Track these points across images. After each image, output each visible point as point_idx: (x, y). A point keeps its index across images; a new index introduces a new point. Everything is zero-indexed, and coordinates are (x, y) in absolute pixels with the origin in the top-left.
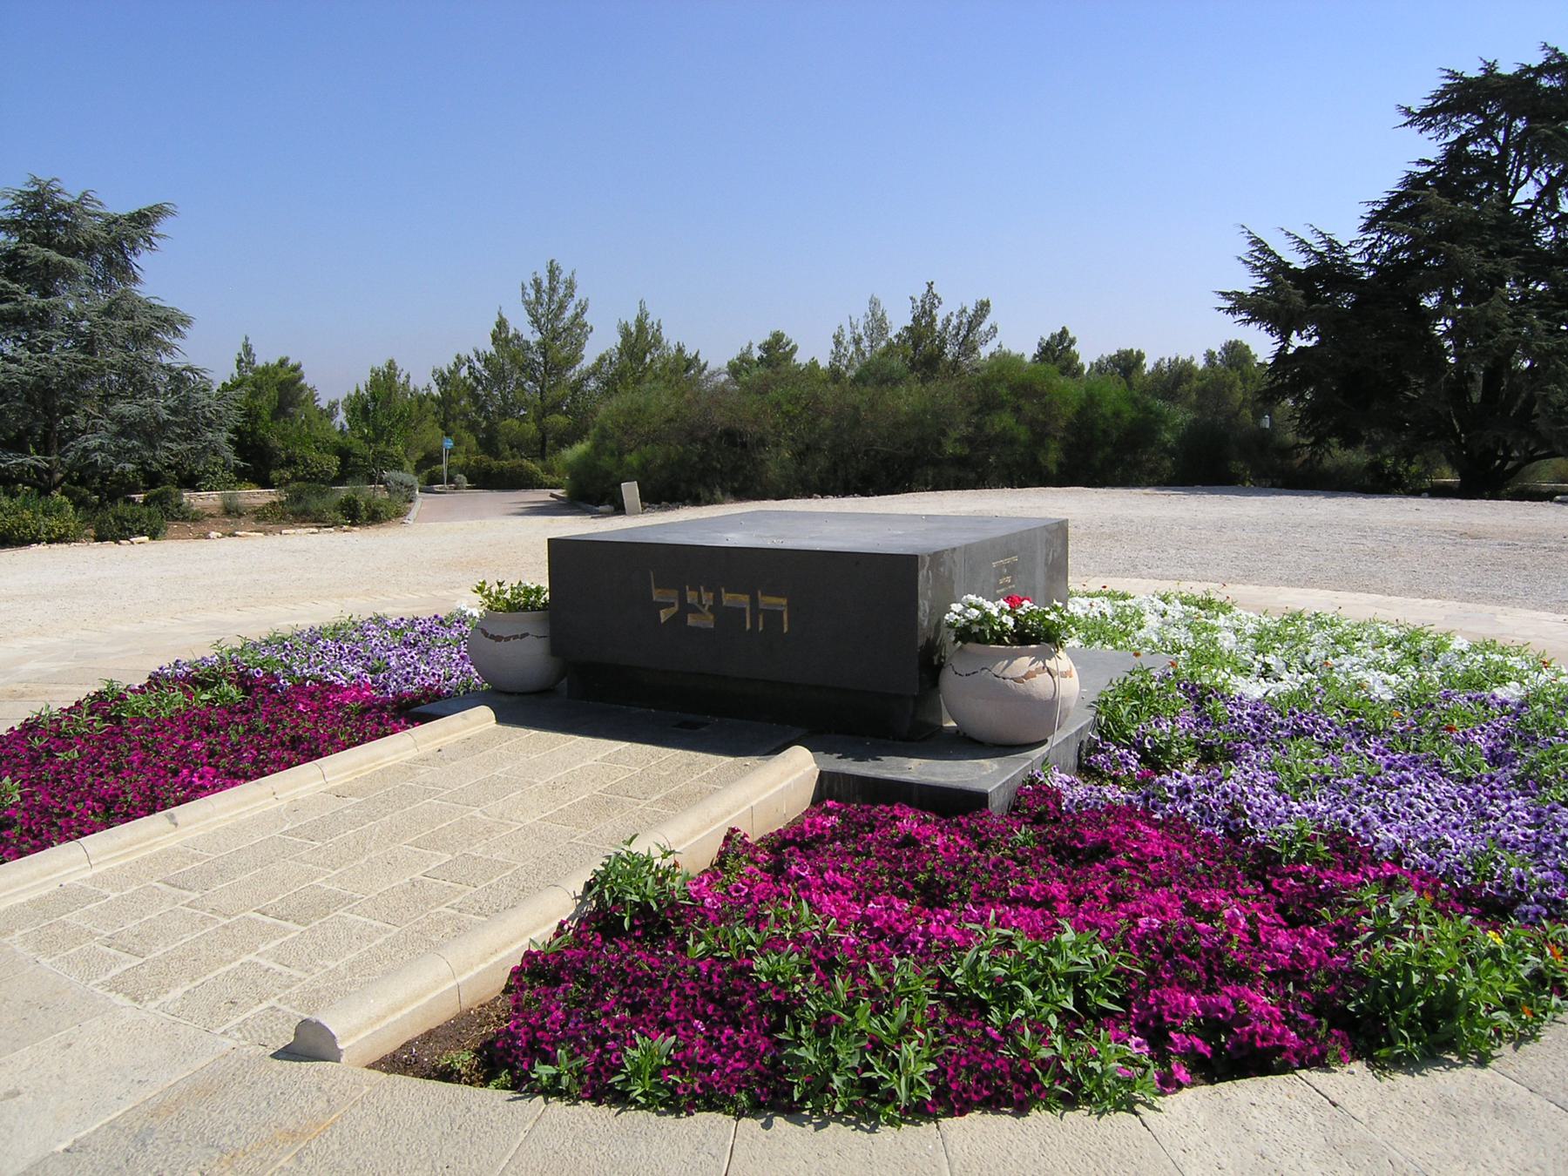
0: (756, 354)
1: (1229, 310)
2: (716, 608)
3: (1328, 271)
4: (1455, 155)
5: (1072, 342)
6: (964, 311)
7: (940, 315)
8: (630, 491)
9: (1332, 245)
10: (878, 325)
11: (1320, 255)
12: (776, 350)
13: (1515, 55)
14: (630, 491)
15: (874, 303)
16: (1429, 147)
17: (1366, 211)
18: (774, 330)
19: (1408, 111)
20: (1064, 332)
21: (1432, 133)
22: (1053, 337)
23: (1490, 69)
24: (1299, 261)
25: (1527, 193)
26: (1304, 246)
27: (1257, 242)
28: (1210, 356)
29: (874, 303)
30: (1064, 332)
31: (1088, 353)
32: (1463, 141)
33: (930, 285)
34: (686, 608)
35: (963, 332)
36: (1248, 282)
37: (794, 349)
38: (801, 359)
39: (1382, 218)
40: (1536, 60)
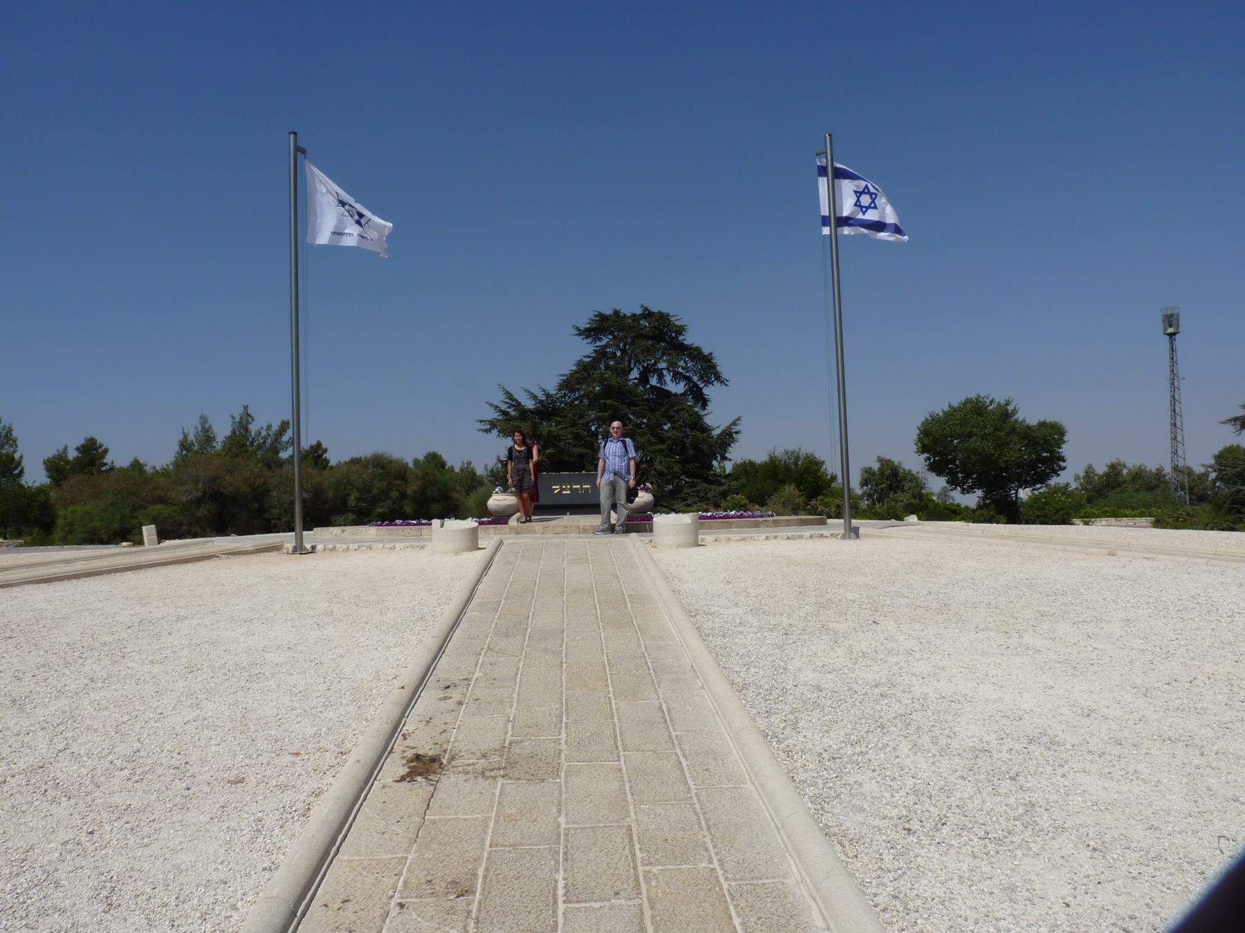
0: (72, 454)
1: (486, 431)
2: (571, 489)
3: (547, 410)
4: (601, 354)
5: (325, 451)
6: (269, 427)
7: (253, 428)
8: (149, 531)
9: (548, 395)
10: (207, 437)
11: (541, 402)
12: (91, 453)
13: (630, 308)
14: (149, 531)
15: (204, 420)
16: (585, 349)
17: (558, 380)
18: (89, 436)
19: (578, 329)
20: (319, 445)
21: (589, 340)
22: (312, 447)
23: (616, 313)
24: (529, 404)
25: (635, 374)
26: (534, 397)
27: (507, 393)
28: (416, 462)
29: (204, 420)
30: (319, 445)
31: (336, 456)
32: (606, 346)
33: (246, 408)
34: (562, 490)
35: (269, 441)
36: (493, 415)
37: (106, 451)
38: (118, 457)
39: (568, 384)
40: (639, 311)
